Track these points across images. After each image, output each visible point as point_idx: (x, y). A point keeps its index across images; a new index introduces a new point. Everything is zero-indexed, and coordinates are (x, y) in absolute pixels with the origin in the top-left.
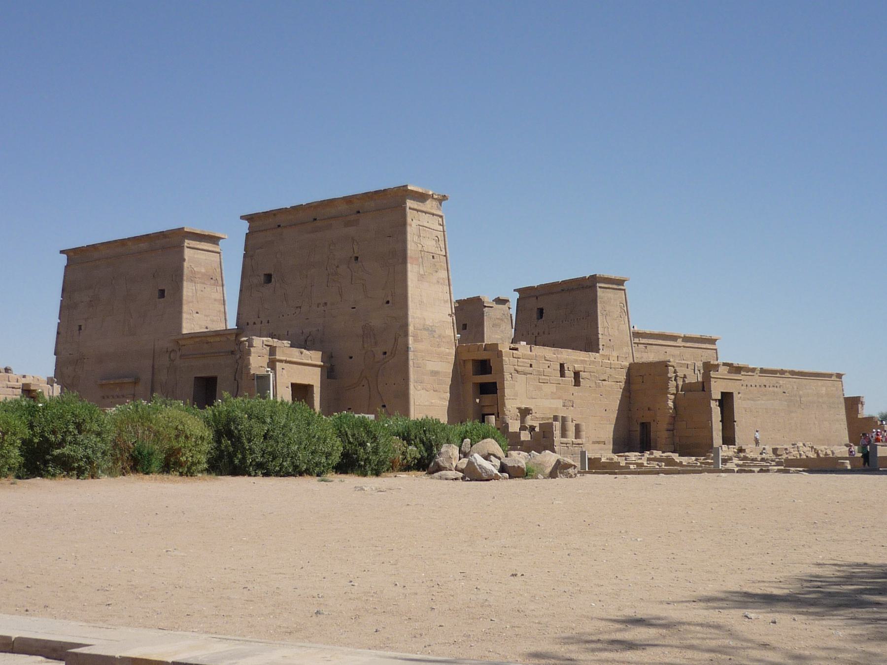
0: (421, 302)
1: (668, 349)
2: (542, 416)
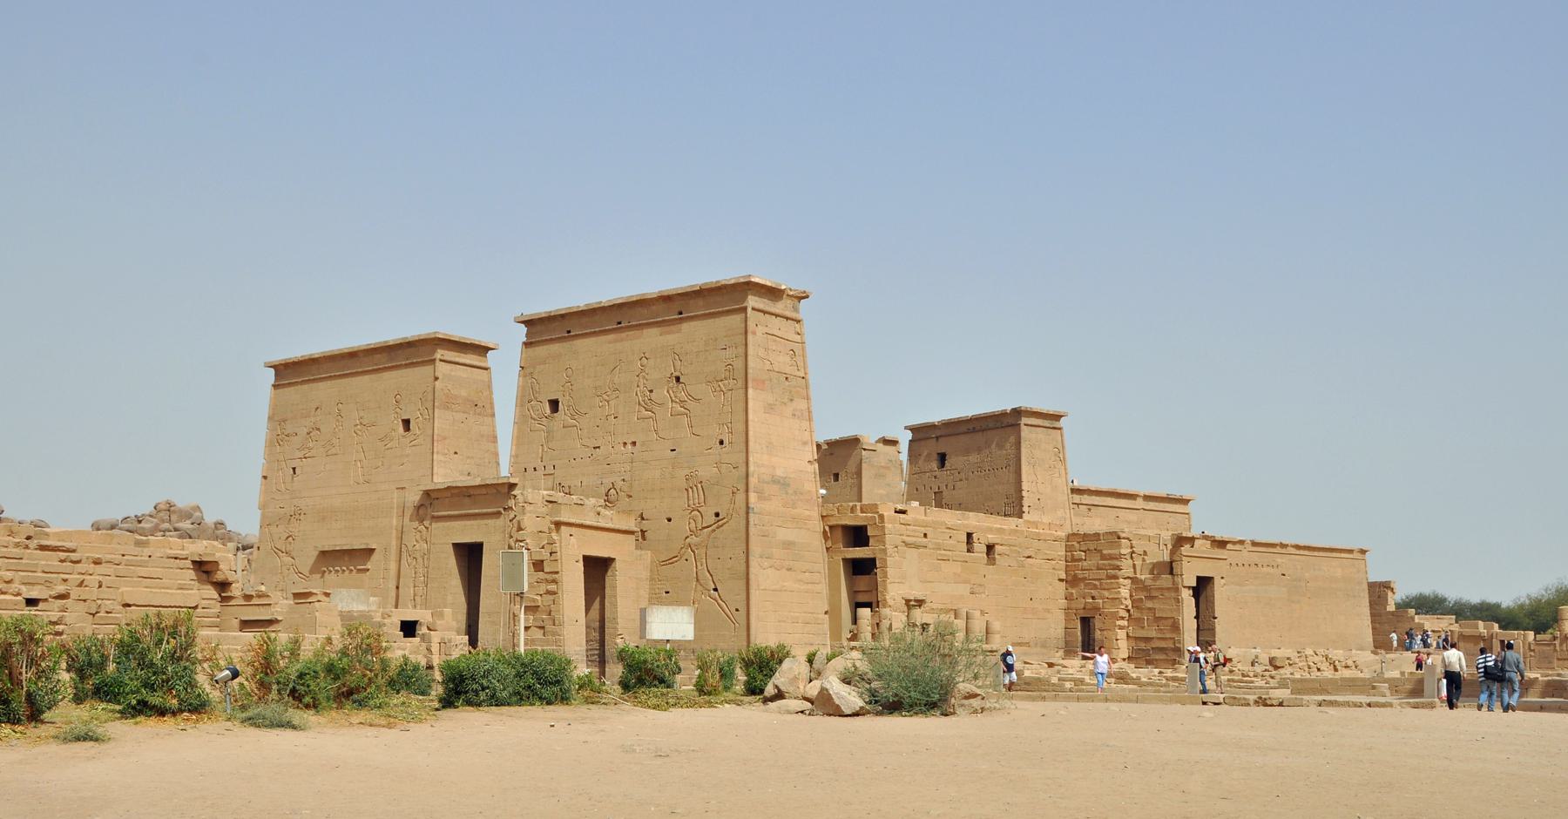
1: (1121, 513)
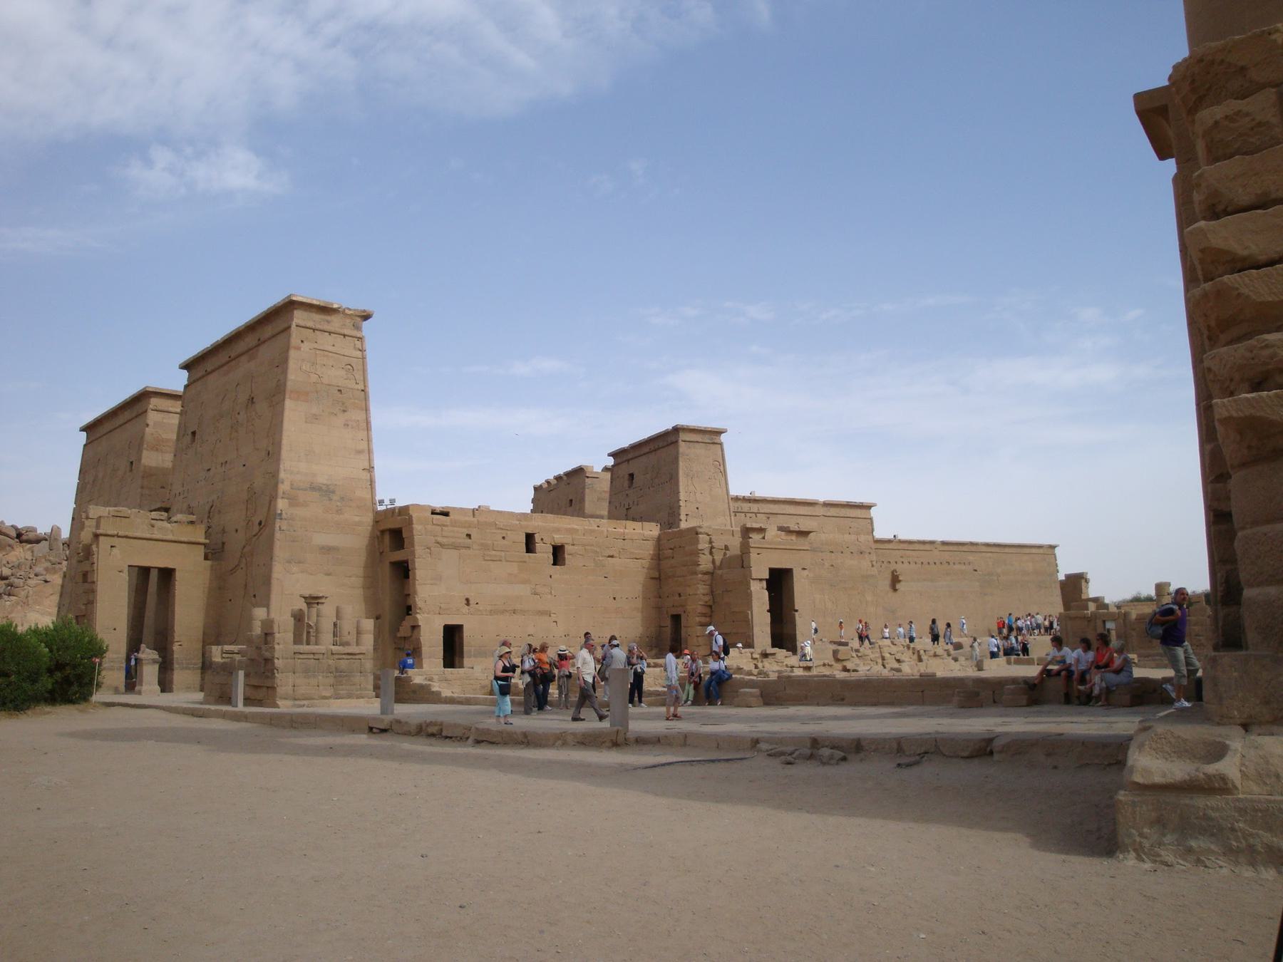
2: (489, 608)
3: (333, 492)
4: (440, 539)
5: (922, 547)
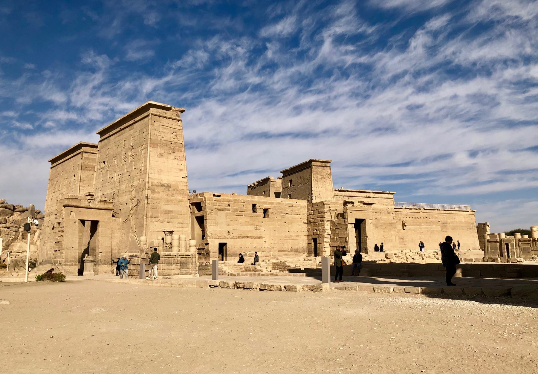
0: (160, 171)
3: (170, 187)
4: (217, 207)
5: (415, 211)
